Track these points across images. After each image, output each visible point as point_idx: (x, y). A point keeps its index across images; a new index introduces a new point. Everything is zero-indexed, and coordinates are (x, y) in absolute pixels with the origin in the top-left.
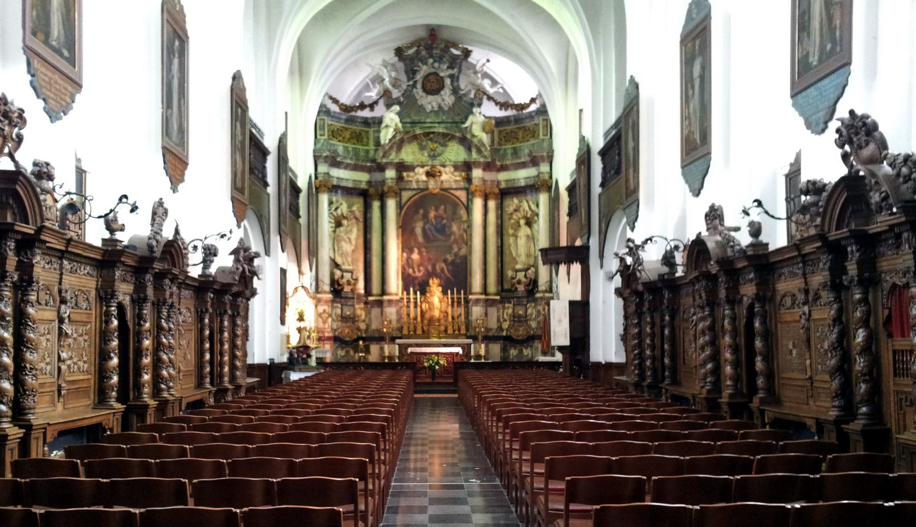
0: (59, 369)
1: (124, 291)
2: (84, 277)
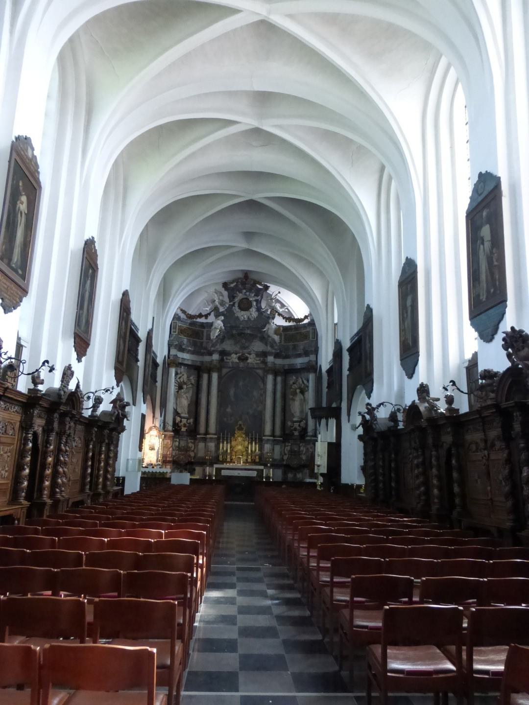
1: (39, 424)
2: (13, 413)
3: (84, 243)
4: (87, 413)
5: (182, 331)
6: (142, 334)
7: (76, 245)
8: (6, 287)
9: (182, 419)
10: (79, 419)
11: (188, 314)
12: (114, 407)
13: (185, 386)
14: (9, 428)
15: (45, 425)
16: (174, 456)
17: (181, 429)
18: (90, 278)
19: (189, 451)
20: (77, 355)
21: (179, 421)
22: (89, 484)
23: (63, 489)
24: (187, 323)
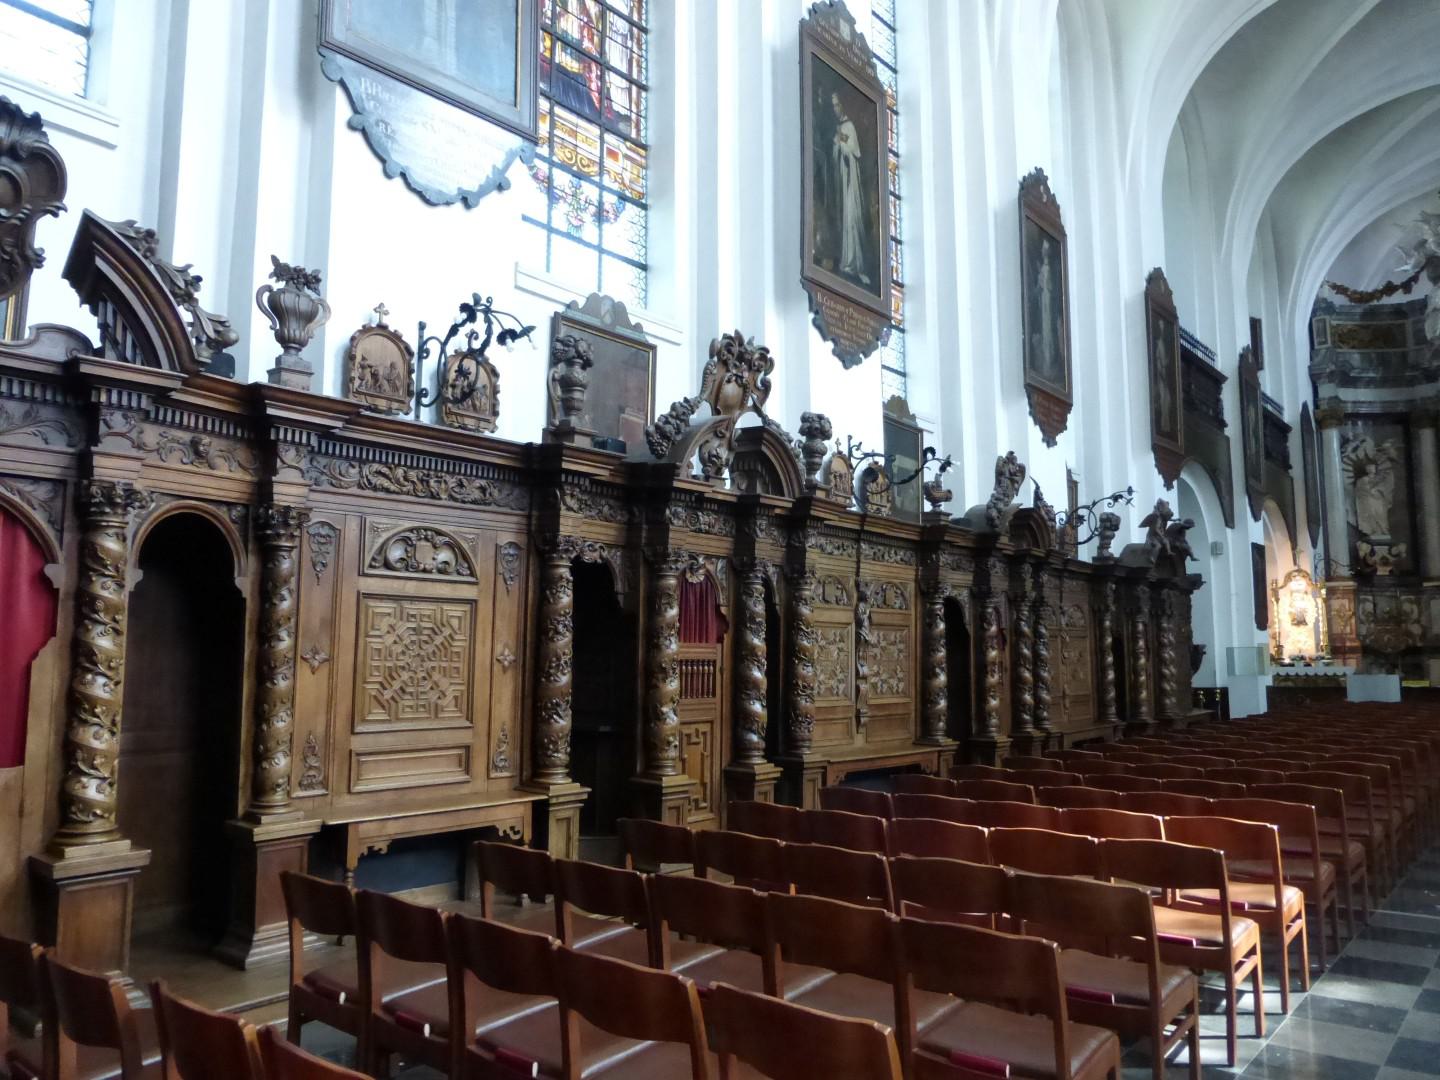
0: (858, 689)
1: (956, 582)
2: (895, 565)
3: (1018, 186)
4: (1086, 554)
5: (1343, 338)
6: (1225, 362)
7: (1001, 195)
8: (836, 315)
9: (1376, 548)
10: (1069, 568)
11: (1355, 292)
12: (1152, 534)
13: (1372, 468)
14: (890, 594)
15: (974, 585)
16: (1365, 637)
17: (1376, 570)
18: (1046, 261)
19: (1405, 621)
20: (1042, 430)
21: (1368, 551)
22: (1113, 703)
23: (1045, 714)
24: (1355, 314)
